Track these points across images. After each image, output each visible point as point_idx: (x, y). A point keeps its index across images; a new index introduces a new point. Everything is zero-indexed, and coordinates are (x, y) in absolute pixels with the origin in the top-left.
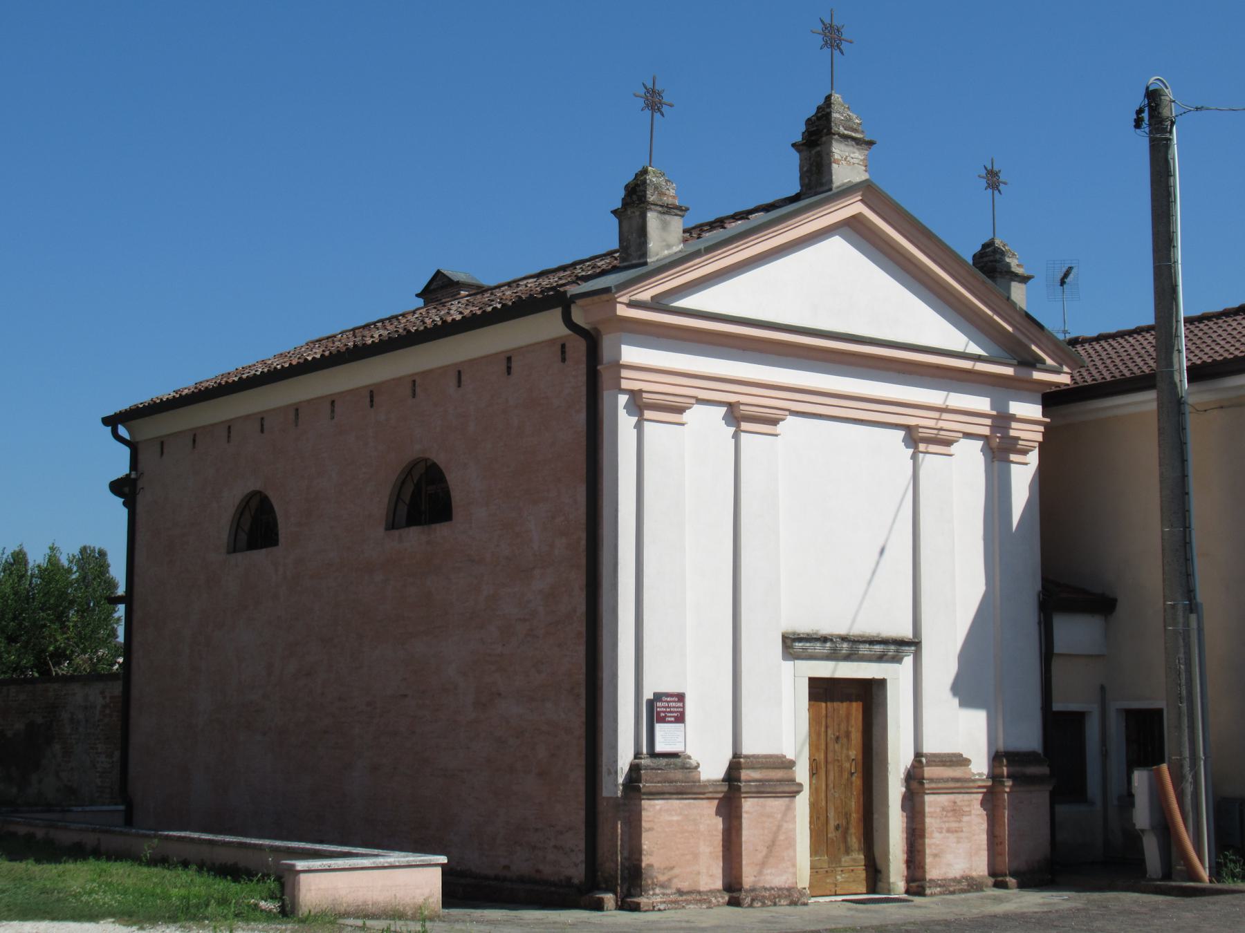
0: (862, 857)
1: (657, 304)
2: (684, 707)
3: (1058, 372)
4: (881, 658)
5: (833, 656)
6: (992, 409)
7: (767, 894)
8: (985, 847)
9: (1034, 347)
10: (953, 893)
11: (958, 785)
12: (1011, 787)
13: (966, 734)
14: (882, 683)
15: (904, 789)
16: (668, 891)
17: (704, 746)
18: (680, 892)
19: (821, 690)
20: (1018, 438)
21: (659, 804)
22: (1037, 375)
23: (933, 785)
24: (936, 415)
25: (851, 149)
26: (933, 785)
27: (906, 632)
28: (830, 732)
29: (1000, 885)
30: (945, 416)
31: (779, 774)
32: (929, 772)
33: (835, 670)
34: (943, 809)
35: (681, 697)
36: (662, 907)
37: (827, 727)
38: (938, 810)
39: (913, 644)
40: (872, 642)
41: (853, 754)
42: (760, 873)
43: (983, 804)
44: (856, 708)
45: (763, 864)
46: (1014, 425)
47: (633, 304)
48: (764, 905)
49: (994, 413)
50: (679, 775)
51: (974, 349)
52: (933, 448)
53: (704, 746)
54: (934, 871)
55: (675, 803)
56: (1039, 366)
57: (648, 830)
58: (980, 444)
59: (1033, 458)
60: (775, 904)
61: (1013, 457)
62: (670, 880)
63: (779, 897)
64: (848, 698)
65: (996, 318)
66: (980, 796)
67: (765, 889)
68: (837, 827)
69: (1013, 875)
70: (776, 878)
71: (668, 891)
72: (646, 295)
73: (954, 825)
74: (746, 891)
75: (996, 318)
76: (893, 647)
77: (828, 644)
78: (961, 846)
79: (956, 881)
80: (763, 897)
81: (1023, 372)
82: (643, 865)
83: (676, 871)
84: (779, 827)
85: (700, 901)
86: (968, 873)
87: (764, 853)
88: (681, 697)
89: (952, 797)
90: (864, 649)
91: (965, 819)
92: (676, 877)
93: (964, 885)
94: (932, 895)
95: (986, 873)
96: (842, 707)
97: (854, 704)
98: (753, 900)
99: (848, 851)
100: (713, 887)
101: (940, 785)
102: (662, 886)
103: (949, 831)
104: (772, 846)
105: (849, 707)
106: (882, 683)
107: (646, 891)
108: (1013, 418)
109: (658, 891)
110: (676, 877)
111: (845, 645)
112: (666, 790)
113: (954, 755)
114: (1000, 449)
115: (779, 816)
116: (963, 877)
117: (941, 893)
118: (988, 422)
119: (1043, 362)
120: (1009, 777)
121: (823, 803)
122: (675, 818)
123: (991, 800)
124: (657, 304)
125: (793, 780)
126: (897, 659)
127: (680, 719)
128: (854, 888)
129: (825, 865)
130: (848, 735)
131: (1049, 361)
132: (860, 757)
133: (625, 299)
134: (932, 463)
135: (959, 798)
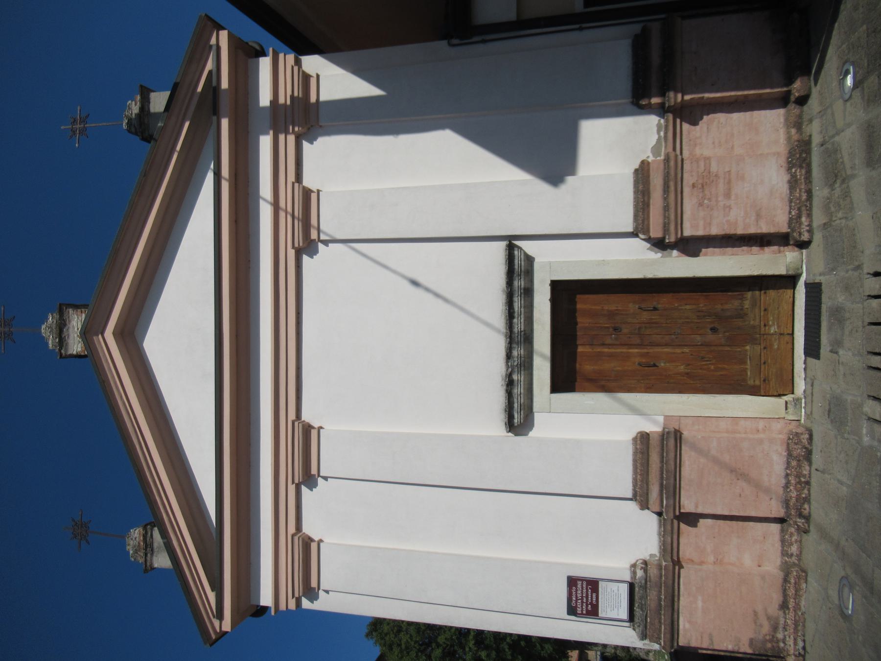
0: (749, 294)
1: (217, 586)
2: (582, 580)
3: (218, 48)
4: (528, 292)
5: (527, 365)
6: (268, 133)
7: (794, 494)
8: (748, 114)
9: (199, 89)
10: (809, 192)
11: (672, 184)
12: (676, 92)
13: (615, 146)
14: (557, 287)
15: (675, 253)
16: (782, 621)
17: (624, 543)
18: (784, 606)
19: (564, 380)
20: (292, 97)
21: (683, 624)
22: (225, 84)
23: (672, 227)
24: (282, 215)
25: (71, 330)
26: (672, 227)
27: (503, 244)
28: (609, 341)
29: (802, 101)
30: (282, 204)
31: (655, 458)
32: (656, 232)
33: (542, 356)
34: (701, 204)
35: (572, 582)
36: (801, 644)
37: (603, 345)
38: (702, 214)
39: (511, 243)
40: (510, 315)
41: (632, 307)
42: (767, 491)
43: (694, 123)
44: (584, 303)
45: (757, 486)
46: (281, 100)
47: (220, 615)
48: (807, 500)
49: (271, 132)
50: (652, 595)
51: (210, 177)
52: (314, 221)
53: (624, 543)
54: (779, 222)
55: (684, 602)
56: (214, 84)
57: (712, 643)
58: (306, 145)
59: (313, 63)
60: (808, 483)
61: (313, 99)
62: (769, 618)
63: (798, 476)
64: (572, 313)
65: (178, 148)
66: (686, 126)
67: (786, 486)
68: (714, 330)
69: (790, 81)
70: (774, 467)
71: (782, 621)
72: (212, 596)
73: (721, 187)
74: (788, 513)
75: (178, 148)
76: (516, 283)
77: (515, 377)
78: (746, 157)
79: (793, 183)
80: (798, 498)
81: (225, 103)
82: (750, 651)
83: (759, 608)
84: (716, 461)
85: (797, 590)
86: (783, 161)
87: (744, 484)
88: (572, 582)
89: (686, 190)
90: (519, 324)
91: (714, 168)
92: (766, 610)
93: (800, 173)
94: (811, 231)
95: (781, 111)
96: (582, 321)
97: (579, 306)
98: (801, 515)
99: (741, 315)
100: (777, 537)
101: (672, 217)
102: (775, 628)
103: (728, 195)
104: (739, 474)
105: (582, 336)
106: (557, 287)
107: (780, 650)
108: (274, 101)
109: (780, 636)
110: (766, 610)
111: (515, 353)
112: (669, 621)
113: (636, 183)
114: (306, 117)
115: (703, 460)
116: (789, 169)
117: (809, 216)
118: (282, 137)
119: (210, 72)
120: (663, 94)
121: (686, 350)
122: (700, 604)
123: (690, 114)
124: (217, 586)
125: (664, 436)
126: (530, 260)
127: (593, 585)
128: (786, 307)
129: (757, 348)
130: (611, 315)
131: (210, 65)
132: (636, 297)
133: (216, 623)
134: (330, 219)
135: (689, 179)
